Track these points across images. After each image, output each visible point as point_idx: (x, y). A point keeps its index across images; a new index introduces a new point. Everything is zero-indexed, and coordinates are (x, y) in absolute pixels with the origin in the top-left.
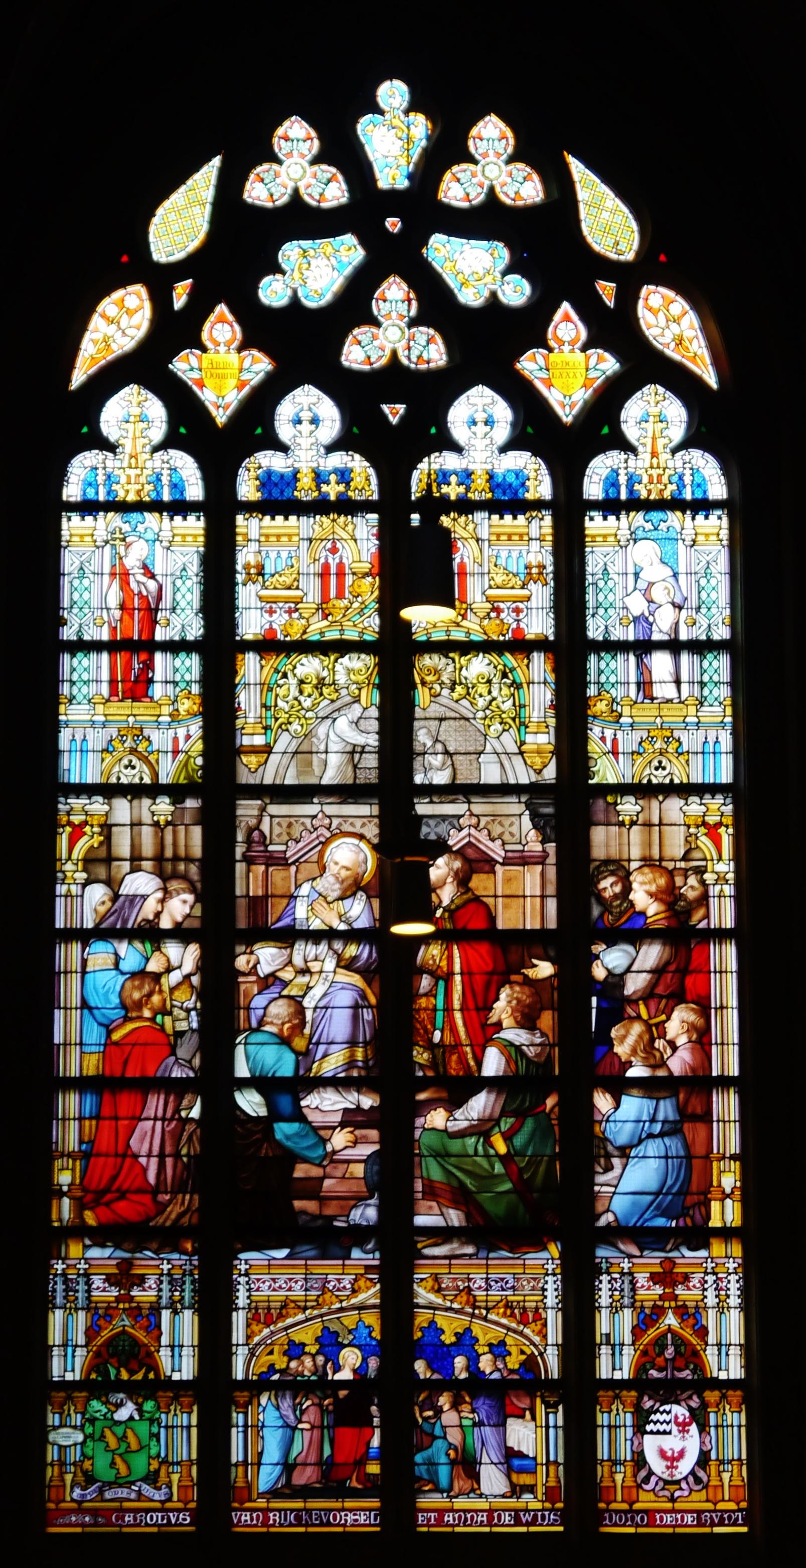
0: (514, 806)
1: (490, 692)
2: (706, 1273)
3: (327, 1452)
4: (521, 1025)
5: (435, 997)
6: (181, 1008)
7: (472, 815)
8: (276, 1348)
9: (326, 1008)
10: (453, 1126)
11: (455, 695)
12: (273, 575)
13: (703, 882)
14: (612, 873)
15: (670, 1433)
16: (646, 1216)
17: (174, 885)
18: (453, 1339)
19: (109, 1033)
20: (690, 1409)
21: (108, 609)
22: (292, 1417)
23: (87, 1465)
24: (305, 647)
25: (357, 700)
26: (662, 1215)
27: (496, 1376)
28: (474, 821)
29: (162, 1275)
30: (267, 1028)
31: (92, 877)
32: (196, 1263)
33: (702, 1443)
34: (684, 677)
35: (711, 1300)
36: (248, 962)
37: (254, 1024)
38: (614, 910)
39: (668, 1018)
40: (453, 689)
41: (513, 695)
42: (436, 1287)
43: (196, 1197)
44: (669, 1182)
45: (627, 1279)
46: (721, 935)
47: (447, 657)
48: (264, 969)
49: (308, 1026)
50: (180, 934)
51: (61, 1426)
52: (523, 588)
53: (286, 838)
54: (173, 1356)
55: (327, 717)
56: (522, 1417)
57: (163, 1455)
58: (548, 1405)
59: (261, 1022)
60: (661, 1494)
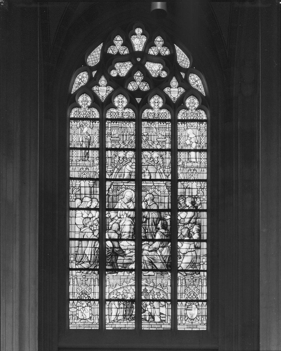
0: (162, 183)
1: (158, 160)
2: (199, 279)
3: (125, 313)
4: (163, 229)
5: (146, 223)
6: (95, 225)
7: (154, 186)
8: (115, 293)
9: (124, 225)
10: (150, 249)
11: (151, 161)
12: (113, 135)
13: (201, 200)
14: (182, 198)
15: (192, 310)
16: (188, 268)
17: (93, 200)
18: (150, 292)
19: (80, 230)
20: (196, 305)
21: (80, 142)
22: (118, 306)
23: (77, 315)
24: (120, 150)
25: (131, 161)
26: (191, 267)
27: (158, 299)
28: (154, 187)
29: (91, 278)
30: (112, 229)
31: (77, 198)
32: (98, 276)
33: (198, 312)
34: (197, 157)
35: (200, 284)
36: (109, 216)
37: (110, 228)
38: (182, 206)
39: (193, 228)
40: (150, 159)
41: (162, 160)
42: (146, 281)
43: (98, 263)
44: (193, 261)
45: (184, 280)
46: (203, 210)
47: (149, 152)
48: (112, 217)
49: (121, 229)
50: (95, 209)
51: (72, 308)
52: (165, 139)
53: (116, 190)
54: (94, 294)
55: (125, 165)
56: (163, 307)
57: (92, 313)
58: (168, 304)
59: (111, 228)
60: (190, 322)
